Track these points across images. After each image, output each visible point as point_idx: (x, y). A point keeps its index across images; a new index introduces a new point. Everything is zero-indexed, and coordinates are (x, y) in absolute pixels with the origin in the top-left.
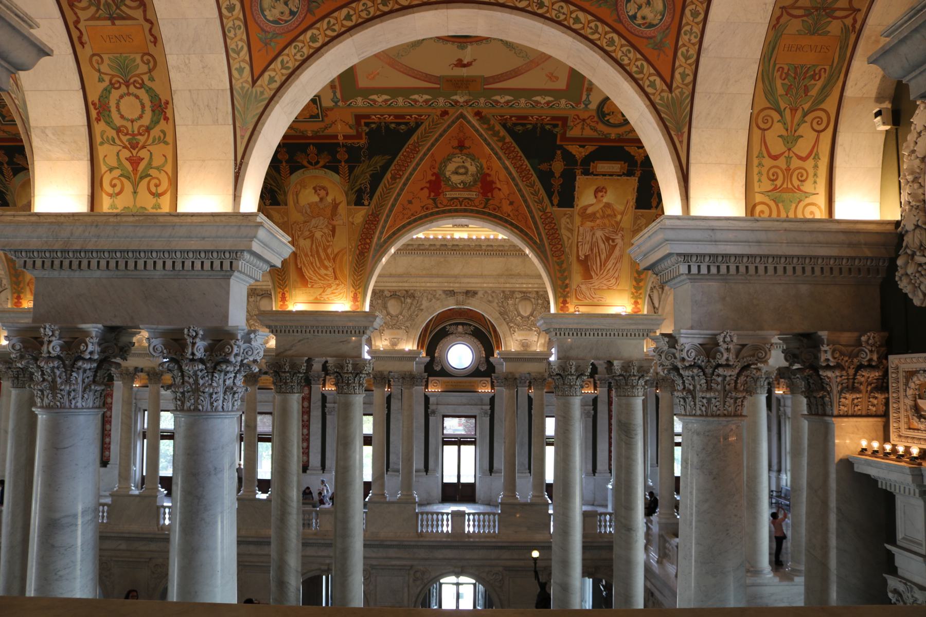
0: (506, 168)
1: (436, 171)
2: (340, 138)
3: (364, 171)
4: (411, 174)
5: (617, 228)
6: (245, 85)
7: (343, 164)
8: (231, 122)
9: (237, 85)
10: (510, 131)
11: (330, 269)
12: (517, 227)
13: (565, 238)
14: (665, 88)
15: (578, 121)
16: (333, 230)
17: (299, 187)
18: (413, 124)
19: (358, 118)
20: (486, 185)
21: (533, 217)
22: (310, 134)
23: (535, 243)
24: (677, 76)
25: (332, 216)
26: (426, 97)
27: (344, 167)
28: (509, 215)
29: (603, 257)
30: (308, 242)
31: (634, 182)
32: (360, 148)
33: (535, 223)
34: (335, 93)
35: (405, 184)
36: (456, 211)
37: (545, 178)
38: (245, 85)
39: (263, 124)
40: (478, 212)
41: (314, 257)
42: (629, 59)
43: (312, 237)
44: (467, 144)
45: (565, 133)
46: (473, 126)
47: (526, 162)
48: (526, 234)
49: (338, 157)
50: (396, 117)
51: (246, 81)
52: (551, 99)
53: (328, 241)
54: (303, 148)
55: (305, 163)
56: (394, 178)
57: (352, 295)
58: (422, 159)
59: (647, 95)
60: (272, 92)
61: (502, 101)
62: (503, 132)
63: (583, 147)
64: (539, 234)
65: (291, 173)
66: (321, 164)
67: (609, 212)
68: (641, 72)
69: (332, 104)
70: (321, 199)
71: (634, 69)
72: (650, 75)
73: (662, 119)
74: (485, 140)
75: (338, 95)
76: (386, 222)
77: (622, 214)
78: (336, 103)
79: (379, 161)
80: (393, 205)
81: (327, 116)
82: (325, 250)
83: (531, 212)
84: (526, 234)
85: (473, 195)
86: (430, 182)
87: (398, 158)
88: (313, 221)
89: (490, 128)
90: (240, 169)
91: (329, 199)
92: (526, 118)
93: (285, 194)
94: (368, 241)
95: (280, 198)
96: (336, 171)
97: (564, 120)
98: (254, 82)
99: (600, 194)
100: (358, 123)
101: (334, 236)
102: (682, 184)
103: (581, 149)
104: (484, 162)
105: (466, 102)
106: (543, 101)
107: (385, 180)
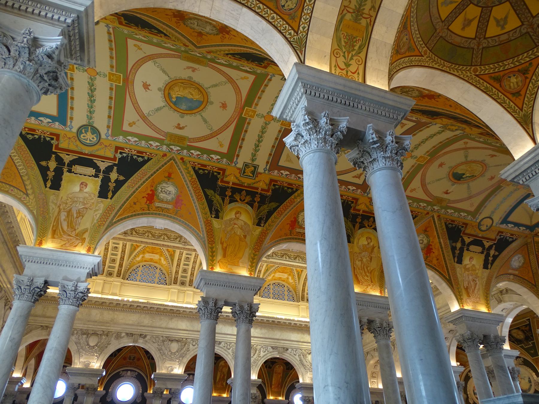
0: (440, 243)
16: (371, 259)
23: (446, 279)
28: (435, 265)
29: (473, 288)
31: (483, 257)
43: (362, 260)
48: (442, 275)
55: (366, 225)
63: (469, 238)
64: (449, 275)
65: (359, 229)
67: (474, 268)
70: (368, 243)
74: (436, 228)
82: (367, 268)
84: (442, 275)
91: (371, 244)
93: (354, 239)
97: (466, 224)
104: (431, 238)
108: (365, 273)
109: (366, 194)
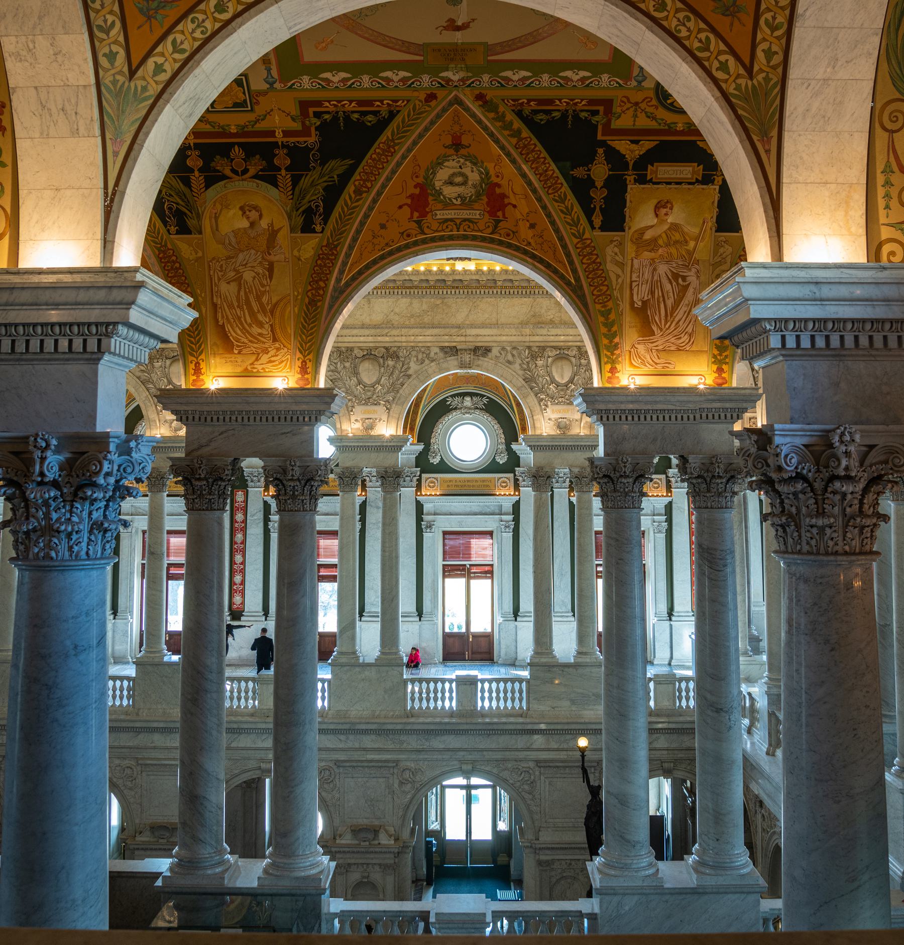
0: (524, 176)
1: (420, 180)
2: (279, 135)
3: (315, 181)
4: (384, 186)
5: (689, 260)
6: (118, 77)
7: (283, 172)
8: (97, 132)
9: (107, 80)
10: (528, 121)
11: (267, 326)
12: (541, 261)
13: (613, 277)
14: (742, 71)
15: (630, 105)
16: (271, 269)
17: (219, 207)
18: (384, 114)
19: (304, 105)
20: (494, 200)
21: (565, 247)
22: (233, 130)
23: (568, 283)
24: (760, 54)
25: (268, 248)
26: (403, 74)
28: (529, 244)
29: (670, 303)
30: (233, 287)
32: (307, 150)
33: (568, 255)
34: (269, 70)
35: (375, 201)
36: (451, 238)
37: (582, 189)
38: (118, 77)
39: (147, 134)
40: (484, 239)
41: (242, 309)
42: (689, 30)
43: (239, 279)
44: (464, 142)
45: (609, 122)
46: (474, 116)
47: (553, 166)
48: (556, 272)
49: (276, 162)
50: (360, 103)
51: (121, 73)
52: (588, 74)
53: (263, 285)
54: (224, 150)
55: (227, 172)
56: (358, 192)
57: (299, 363)
58: (399, 164)
59: (715, 81)
60: (160, 87)
61: (515, 78)
62: (517, 124)
63: (636, 142)
64: (574, 271)
65: (207, 187)
66: (252, 171)
67: (677, 236)
68: (706, 49)
69: (266, 86)
70: (252, 224)
71: (697, 44)
72: (720, 53)
73: (739, 118)
74: (492, 135)
75: (274, 73)
76: (348, 256)
77: (697, 239)
78: (271, 84)
79: (337, 167)
80: (358, 232)
81: (258, 103)
82: (258, 298)
83: (561, 239)
84: (556, 272)
85: (475, 214)
86: (412, 196)
87: (364, 163)
88: (241, 256)
89: (501, 118)
90: (112, 200)
91: (264, 224)
92: (550, 102)
93: (199, 217)
94: (322, 284)
95: (191, 223)
97: (608, 103)
98: (132, 73)
99: (663, 211)
100: (304, 114)
101: (271, 277)
102: (771, 213)
103: (634, 147)
104: (490, 166)
105: (463, 80)
106: (575, 78)
107: (345, 195)
108: (253, 314)
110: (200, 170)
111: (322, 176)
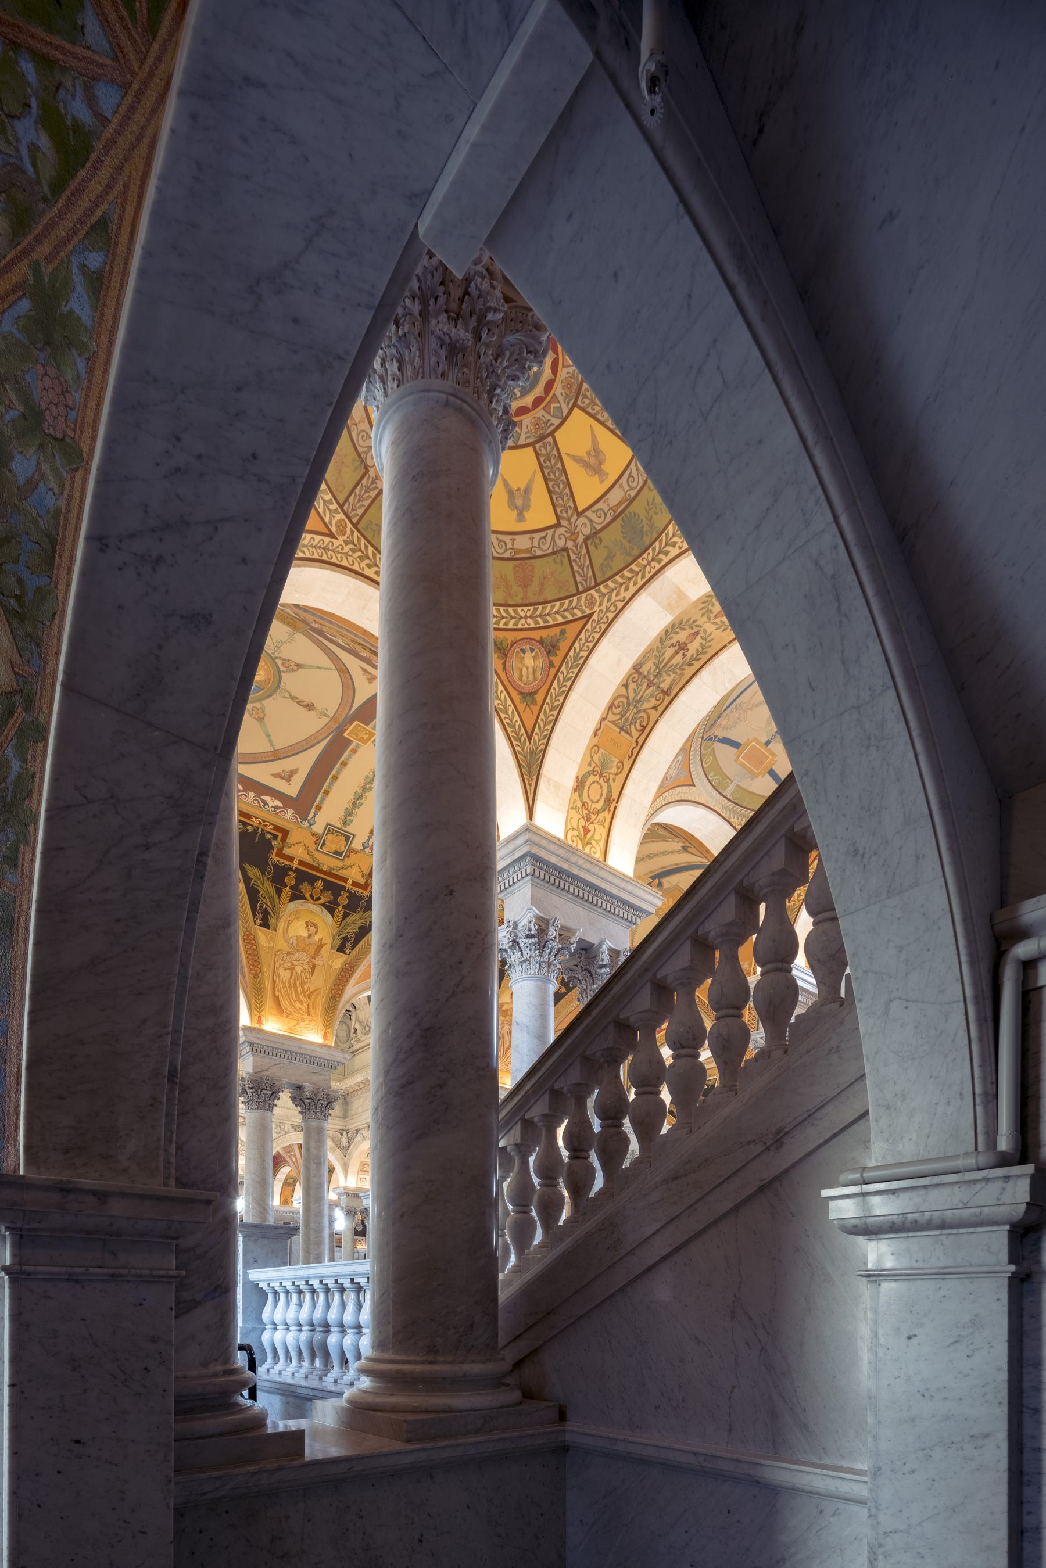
2: (349, 882)
7: (340, 908)
16: (313, 968)
22: (325, 868)
27: (340, 911)
30: (288, 974)
32: (361, 898)
43: (292, 969)
49: (339, 900)
54: (312, 880)
55: (307, 896)
65: (290, 901)
66: (322, 901)
69: (360, 847)
70: (310, 936)
82: (302, 985)
88: (297, 955)
91: (317, 938)
95: (272, 921)
96: (332, 912)
109: (306, 824)
110: (291, 888)
111: (361, 918)
